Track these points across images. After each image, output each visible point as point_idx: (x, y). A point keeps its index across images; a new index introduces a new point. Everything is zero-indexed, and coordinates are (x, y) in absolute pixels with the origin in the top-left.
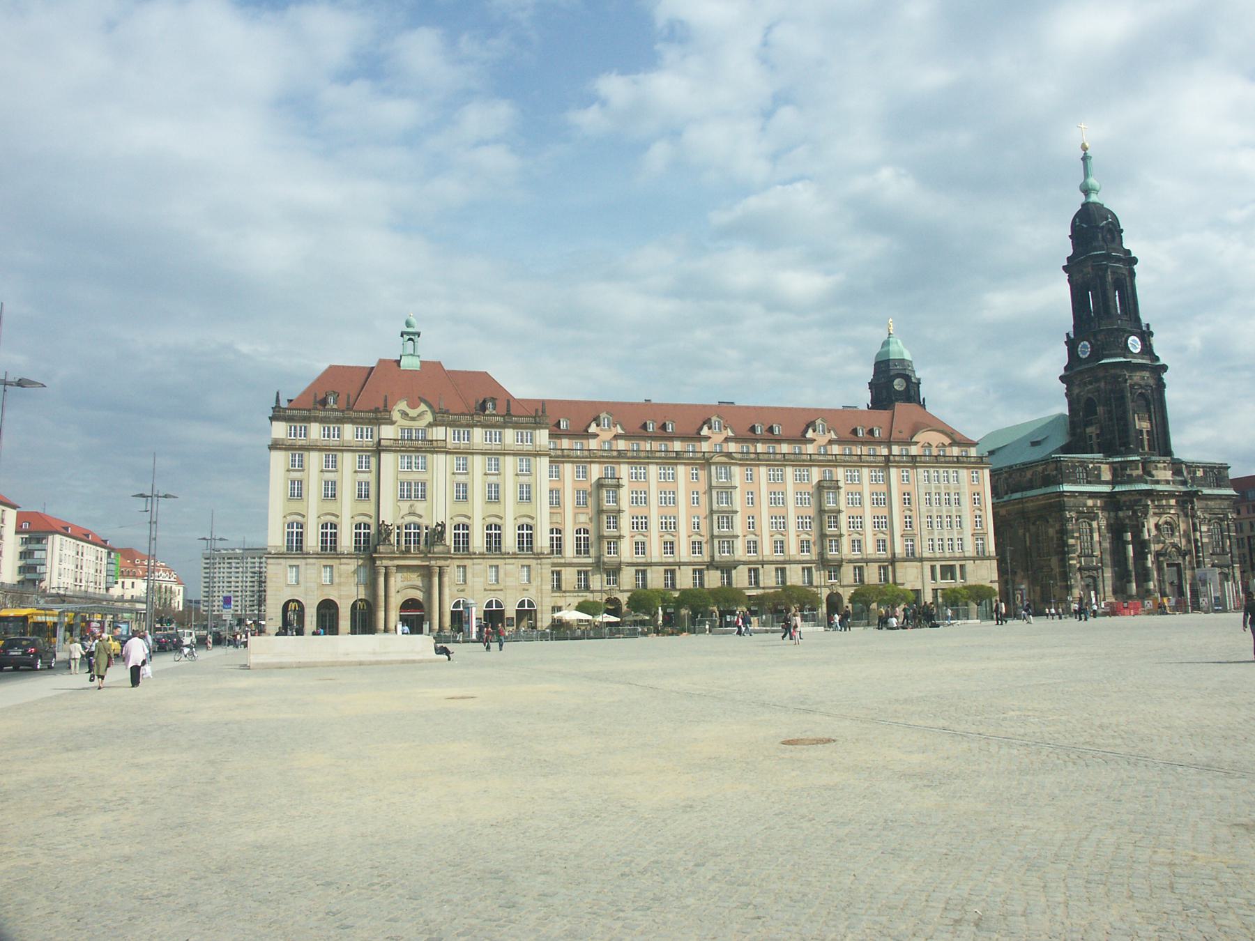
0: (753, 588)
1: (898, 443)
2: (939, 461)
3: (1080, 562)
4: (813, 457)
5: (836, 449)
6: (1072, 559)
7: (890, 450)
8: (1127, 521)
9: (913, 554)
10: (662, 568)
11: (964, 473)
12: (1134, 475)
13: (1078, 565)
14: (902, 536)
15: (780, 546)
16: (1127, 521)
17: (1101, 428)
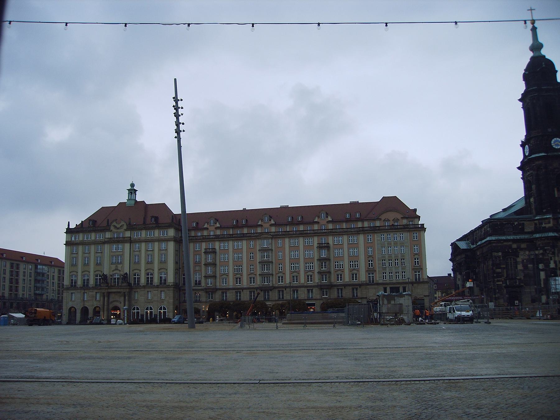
0: (281, 300)
1: (366, 220)
2: (394, 228)
3: (506, 283)
4: (316, 231)
5: (330, 226)
6: (498, 281)
7: (363, 224)
8: (541, 256)
9: (373, 281)
10: (234, 291)
11: (405, 235)
12: (547, 227)
13: (504, 285)
14: (367, 271)
15: (295, 277)
16: (541, 256)
17: (534, 198)
